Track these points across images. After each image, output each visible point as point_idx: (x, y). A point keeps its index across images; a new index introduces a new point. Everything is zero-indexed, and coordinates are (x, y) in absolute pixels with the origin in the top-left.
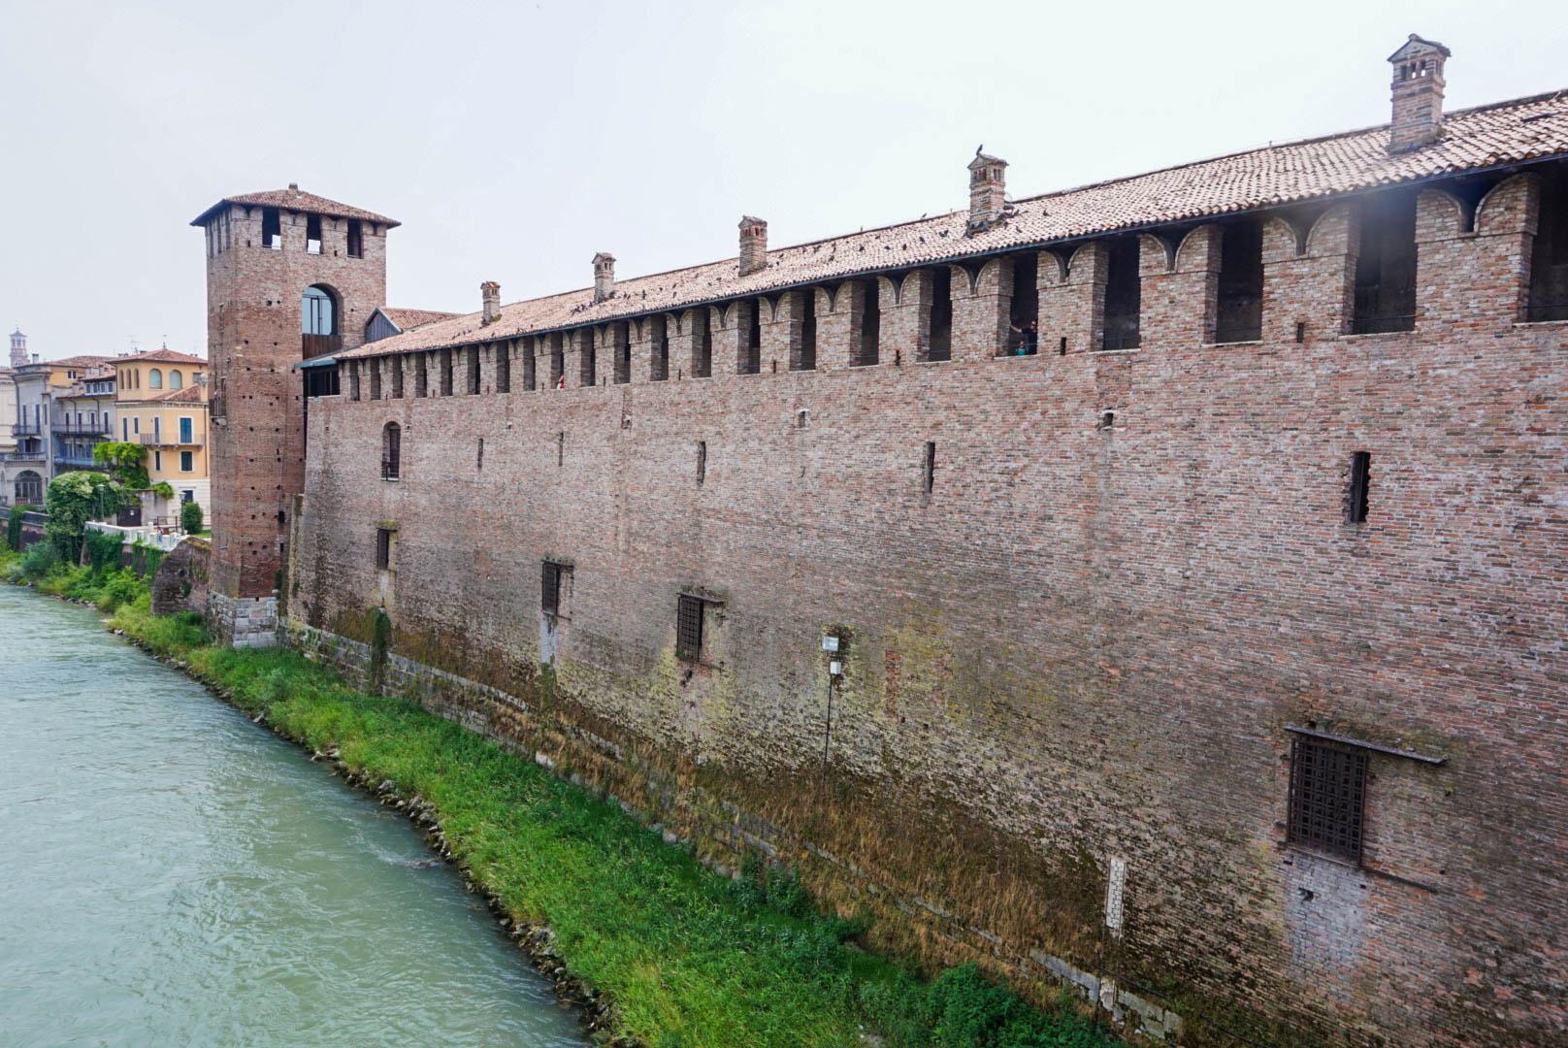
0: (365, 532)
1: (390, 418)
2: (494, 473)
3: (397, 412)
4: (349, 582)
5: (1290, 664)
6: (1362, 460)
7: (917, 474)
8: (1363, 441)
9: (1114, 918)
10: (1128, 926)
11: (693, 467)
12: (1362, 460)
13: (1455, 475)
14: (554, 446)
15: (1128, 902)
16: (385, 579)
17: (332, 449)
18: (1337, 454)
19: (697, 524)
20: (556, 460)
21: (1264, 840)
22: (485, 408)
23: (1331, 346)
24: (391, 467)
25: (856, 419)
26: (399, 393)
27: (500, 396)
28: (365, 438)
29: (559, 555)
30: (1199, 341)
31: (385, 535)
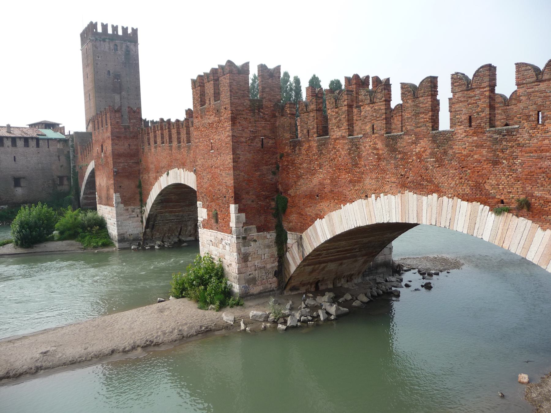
6: (15, 157)
8: (15, 155)
12: (15, 157)
13: (22, 157)
18: (13, 156)
21: (12, 187)
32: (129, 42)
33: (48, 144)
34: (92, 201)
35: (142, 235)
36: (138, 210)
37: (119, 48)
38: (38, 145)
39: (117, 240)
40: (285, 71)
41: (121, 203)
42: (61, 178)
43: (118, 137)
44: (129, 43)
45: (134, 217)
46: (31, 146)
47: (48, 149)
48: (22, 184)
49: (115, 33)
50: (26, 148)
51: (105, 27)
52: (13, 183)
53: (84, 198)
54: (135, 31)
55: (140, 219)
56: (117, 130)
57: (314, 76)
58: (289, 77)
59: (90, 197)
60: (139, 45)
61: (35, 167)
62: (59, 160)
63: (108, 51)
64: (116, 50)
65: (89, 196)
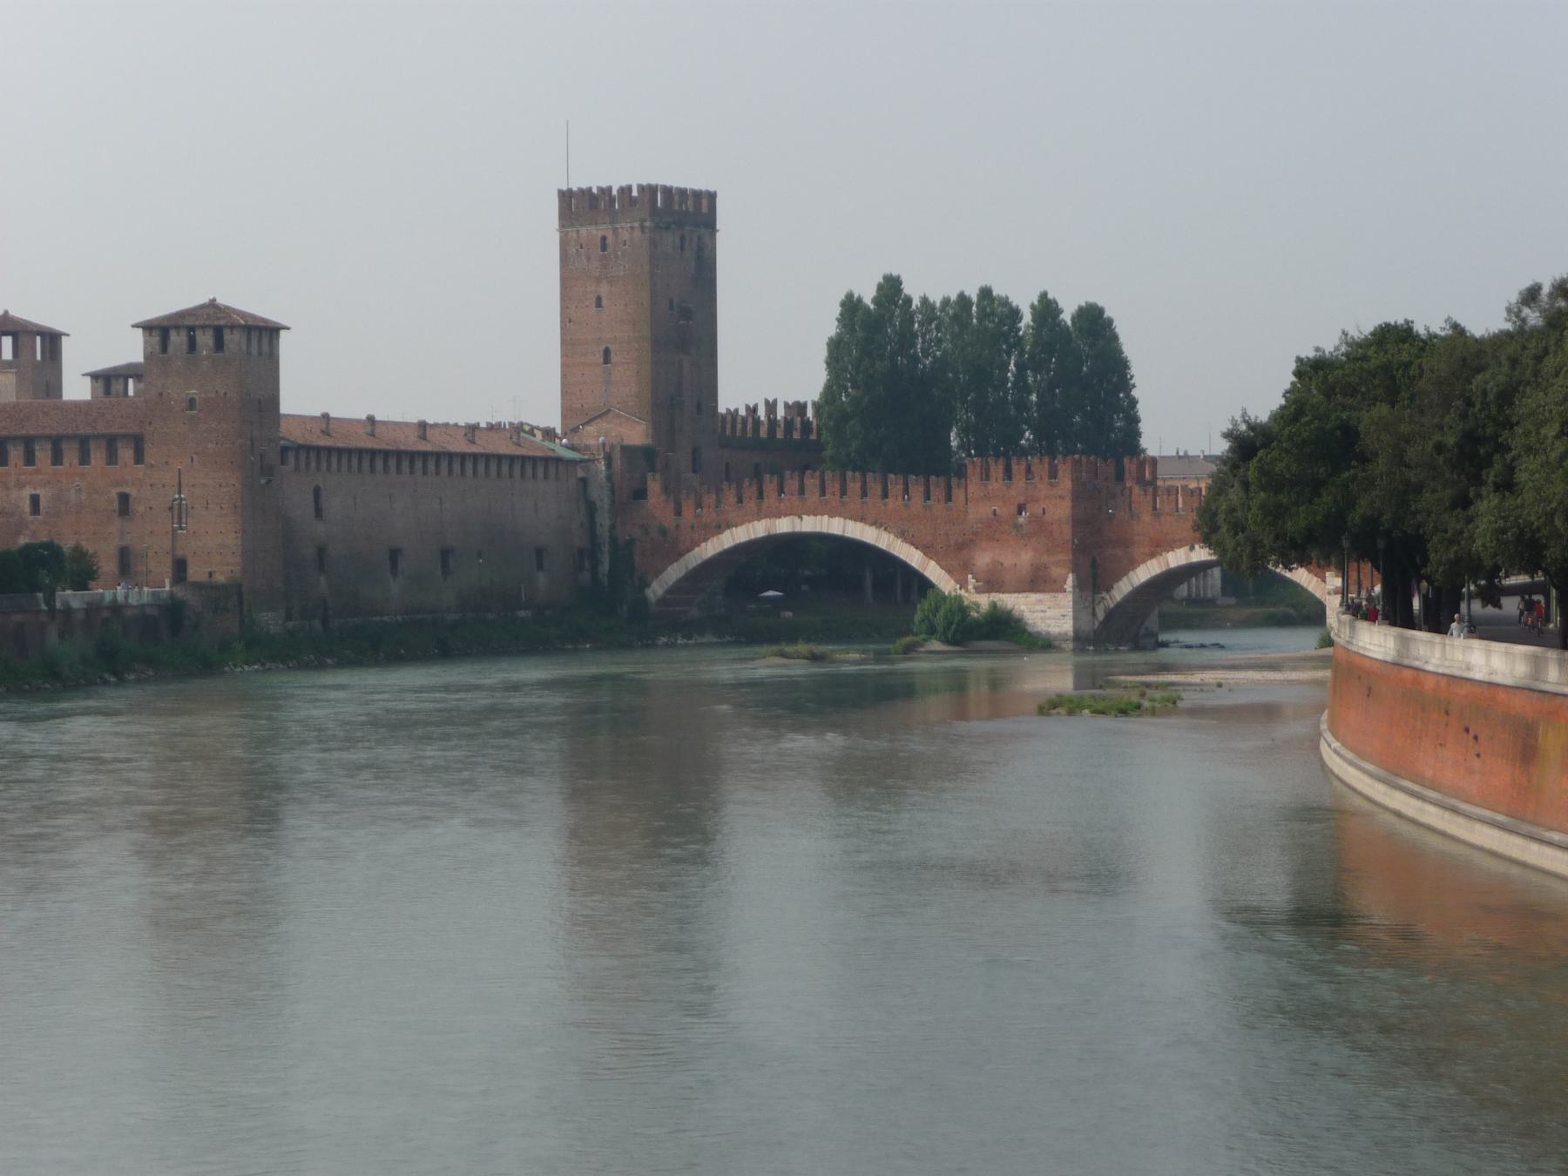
16: (322, 579)
24: (319, 513)
26: (318, 469)
31: (321, 551)
36: (1090, 599)
49: (684, 208)
53: (662, 601)
57: (1044, 296)
60: (717, 234)
64: (682, 248)
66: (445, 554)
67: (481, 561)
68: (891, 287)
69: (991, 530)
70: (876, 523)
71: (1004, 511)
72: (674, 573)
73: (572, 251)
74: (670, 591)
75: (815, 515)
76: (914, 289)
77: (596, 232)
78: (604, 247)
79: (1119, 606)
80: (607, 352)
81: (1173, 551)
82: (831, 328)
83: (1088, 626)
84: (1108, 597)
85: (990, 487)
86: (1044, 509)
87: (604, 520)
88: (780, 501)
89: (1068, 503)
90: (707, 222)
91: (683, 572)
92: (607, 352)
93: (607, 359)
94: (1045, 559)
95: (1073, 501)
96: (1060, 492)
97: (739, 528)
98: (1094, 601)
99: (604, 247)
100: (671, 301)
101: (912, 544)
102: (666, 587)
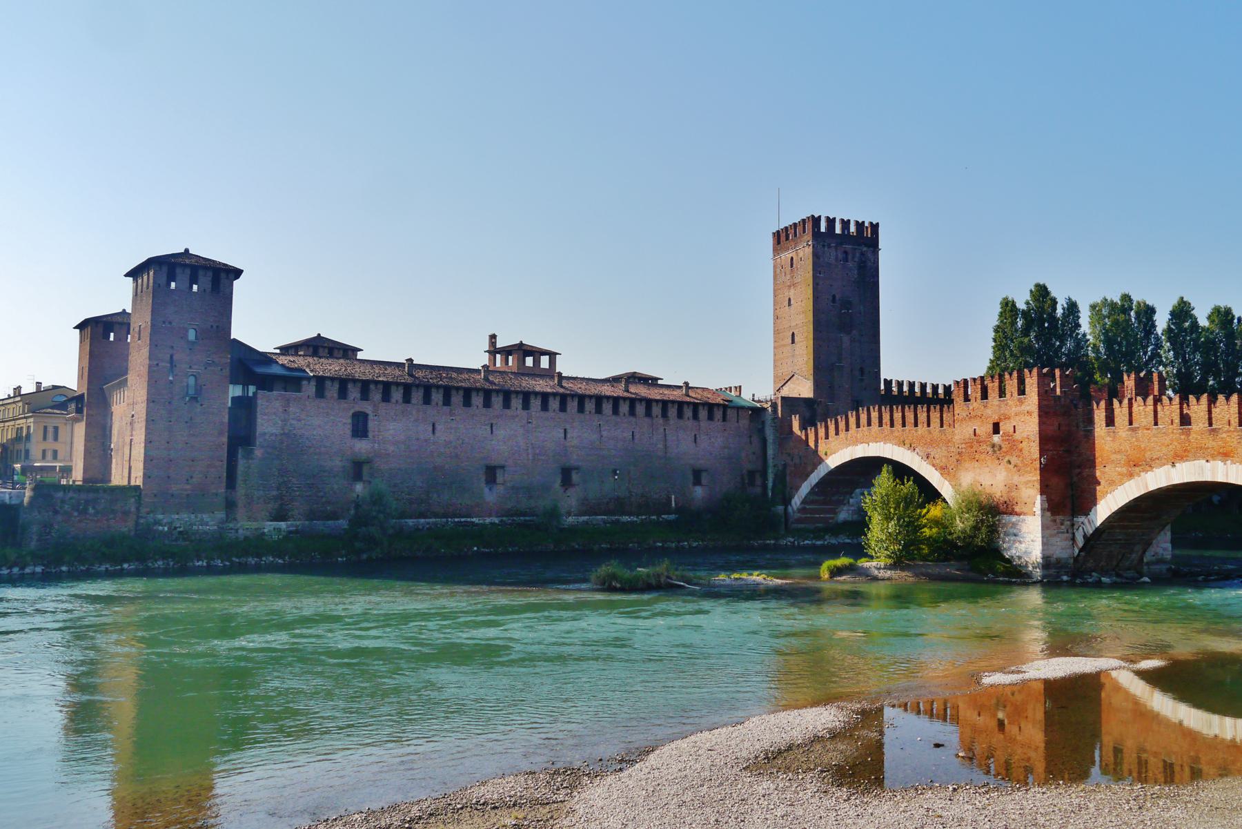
0: (337, 463)
1: (357, 409)
2: (442, 435)
3: (367, 407)
4: (320, 492)
5: (692, 462)
6: (695, 435)
7: (631, 437)
9: (673, 505)
10: (676, 504)
11: (563, 435)
12: (695, 435)
14: (488, 428)
15: (675, 501)
17: (293, 422)
18: (693, 434)
19: (566, 450)
20: (490, 432)
21: (691, 486)
22: (435, 411)
23: (691, 421)
25: (615, 426)
27: (445, 407)
28: (332, 418)
29: (494, 463)
30: (676, 417)
32: (866, 245)
33: (738, 416)
34: (809, 516)
35: (1072, 561)
37: (850, 257)
38: (724, 419)
39: (1040, 566)
40: (1123, 293)
41: (1048, 510)
42: (752, 474)
43: (1046, 413)
44: (865, 249)
45: (1063, 533)
46: (716, 419)
47: (736, 424)
48: (704, 481)
49: (846, 233)
50: (710, 422)
51: (846, 224)
52: (691, 477)
53: (802, 510)
54: (875, 227)
55: (1070, 535)
56: (1046, 403)
58: (1131, 300)
59: (810, 508)
61: (720, 454)
62: (751, 443)
63: (834, 261)
64: (846, 260)
65: (808, 507)
66: (566, 475)
67: (616, 477)
68: (1041, 293)
69: (971, 451)
70: (912, 447)
71: (985, 429)
72: (805, 489)
73: (778, 271)
74: (804, 502)
75: (877, 442)
76: (1061, 296)
77: (786, 256)
78: (792, 266)
79: (1099, 531)
80: (793, 334)
81: (1152, 470)
82: (994, 320)
83: (1062, 550)
84: (1086, 521)
85: (971, 408)
86: (1014, 426)
87: (770, 452)
88: (857, 432)
89: (1035, 419)
90: (873, 243)
91: (810, 488)
92: (793, 334)
93: (793, 342)
94: (1016, 479)
95: (1040, 416)
96: (1028, 408)
97: (837, 454)
98: (1073, 525)
99: (792, 266)
100: (834, 297)
101: (934, 465)
102: (801, 500)
